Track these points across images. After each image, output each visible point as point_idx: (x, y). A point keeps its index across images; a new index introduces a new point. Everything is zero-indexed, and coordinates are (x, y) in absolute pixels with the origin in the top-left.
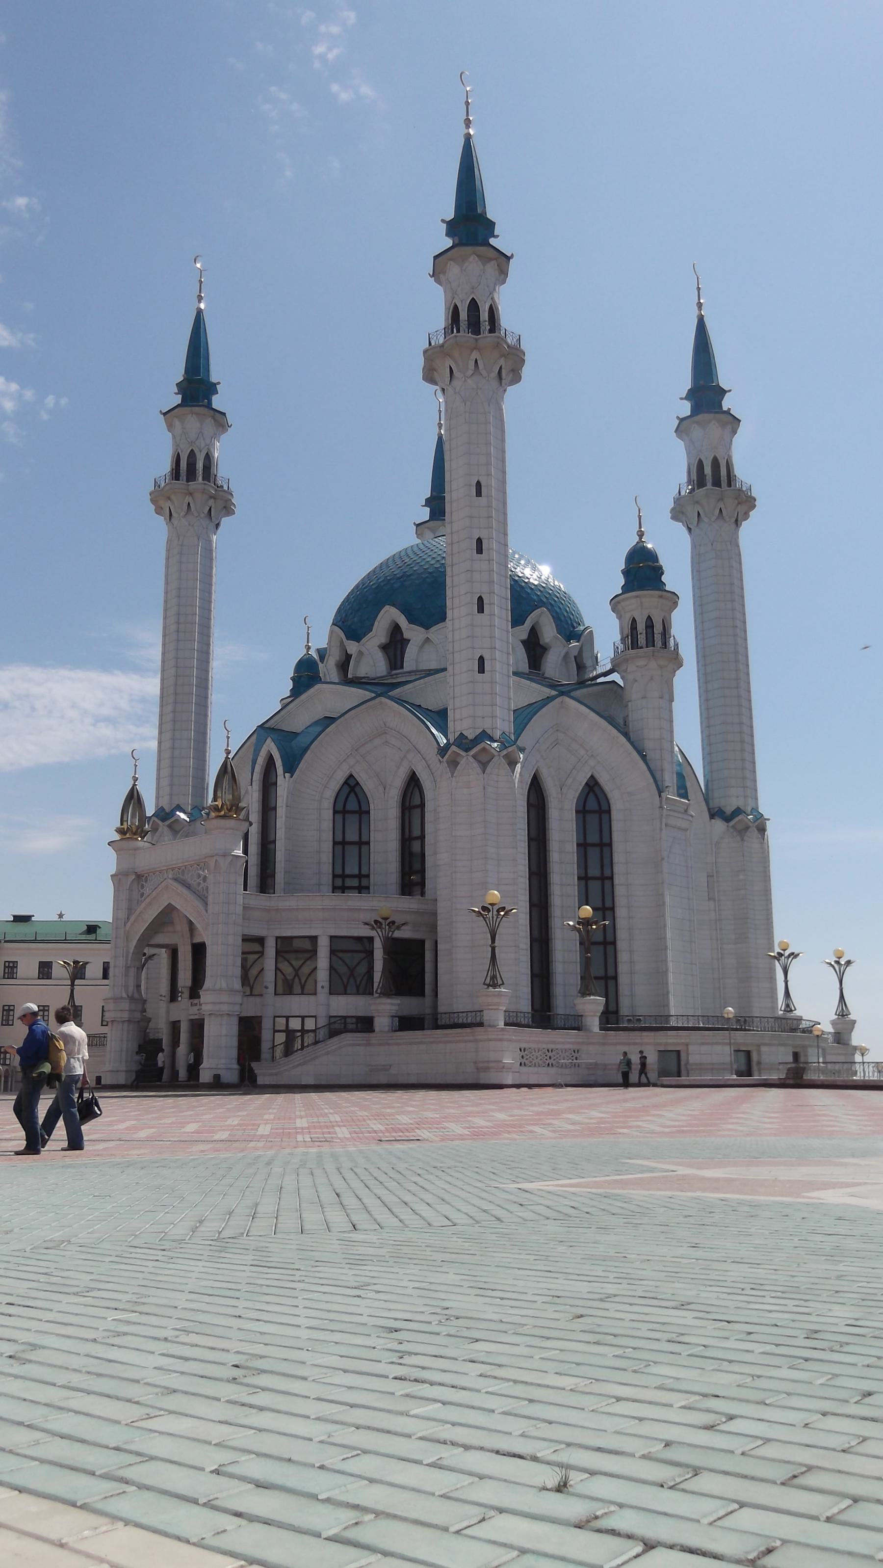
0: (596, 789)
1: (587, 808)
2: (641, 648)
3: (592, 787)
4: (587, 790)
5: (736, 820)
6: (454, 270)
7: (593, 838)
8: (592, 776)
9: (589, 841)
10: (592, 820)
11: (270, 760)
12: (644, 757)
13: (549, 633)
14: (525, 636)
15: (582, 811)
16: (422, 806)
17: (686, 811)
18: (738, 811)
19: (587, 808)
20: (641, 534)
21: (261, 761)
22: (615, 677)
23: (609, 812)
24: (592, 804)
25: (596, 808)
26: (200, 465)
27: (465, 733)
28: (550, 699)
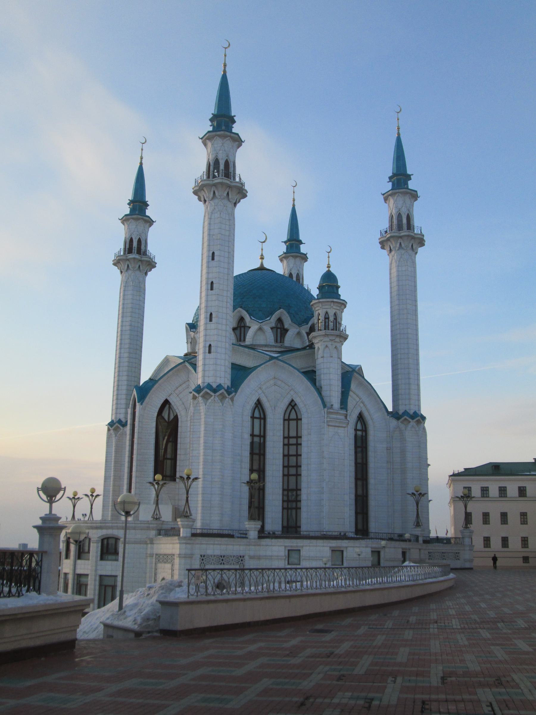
1: (291, 417)
2: (320, 330)
3: (292, 405)
4: (290, 407)
5: (403, 419)
6: (209, 144)
7: (293, 433)
8: (292, 400)
9: (291, 435)
12: (319, 390)
13: (287, 322)
14: (273, 325)
15: (287, 420)
17: (346, 417)
18: (405, 413)
19: (291, 417)
20: (329, 267)
24: (293, 416)
25: (295, 417)
26: (135, 244)
28: (269, 360)
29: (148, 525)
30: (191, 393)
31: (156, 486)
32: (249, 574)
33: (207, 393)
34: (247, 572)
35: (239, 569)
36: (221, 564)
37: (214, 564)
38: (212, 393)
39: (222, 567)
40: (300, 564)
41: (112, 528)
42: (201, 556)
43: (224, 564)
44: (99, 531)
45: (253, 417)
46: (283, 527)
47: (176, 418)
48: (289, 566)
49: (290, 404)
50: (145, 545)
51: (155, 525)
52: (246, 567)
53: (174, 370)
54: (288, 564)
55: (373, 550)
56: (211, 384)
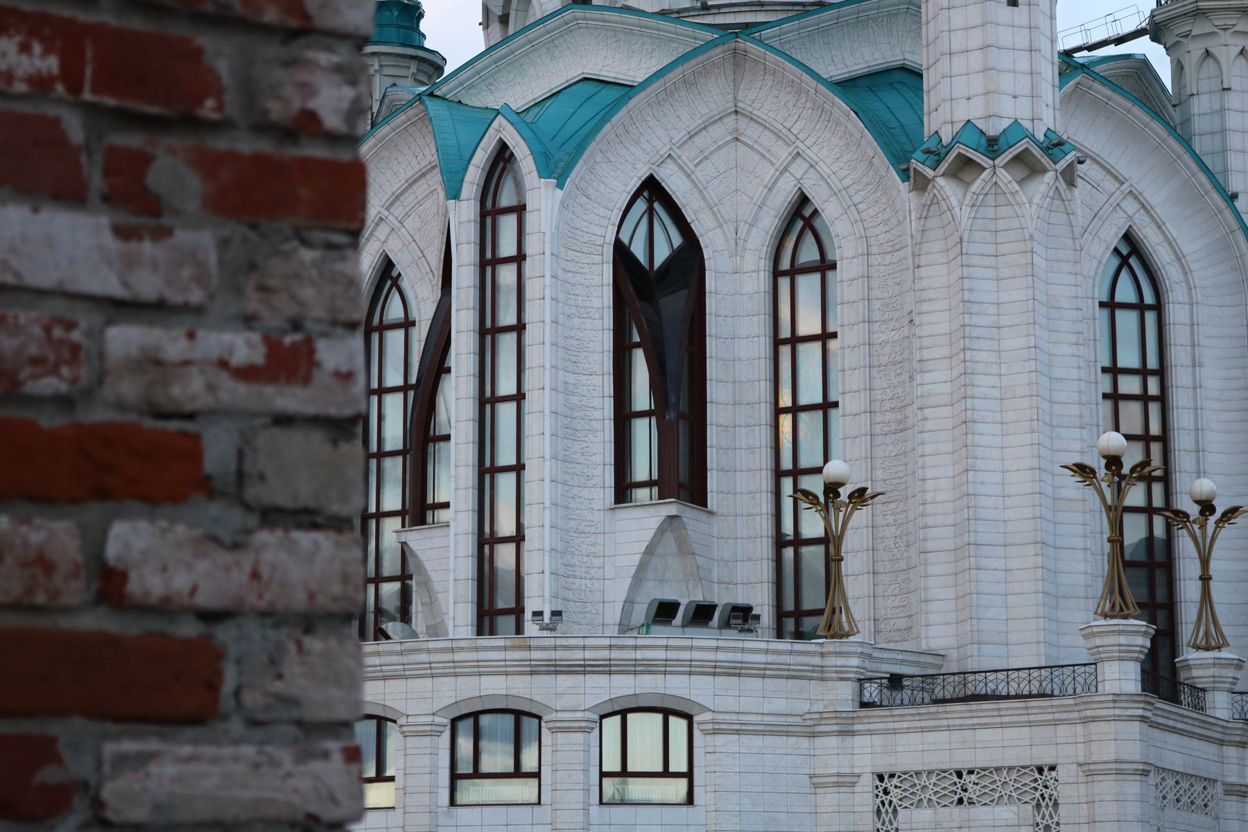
0: (1133, 261)
1: (1120, 297)
4: (1115, 262)
7: (1128, 357)
8: (1128, 237)
10: (1127, 321)
11: (503, 157)
15: (1111, 305)
16: (825, 266)
19: (1120, 297)
21: (481, 158)
22: (1143, 47)
23: (1158, 307)
24: (1125, 293)
25: (1131, 298)
27: (980, 124)
29: (816, 660)
33: (969, 162)
38: (1045, 160)
41: (665, 668)
44: (601, 680)
49: (1116, 251)
50: (805, 742)
51: (854, 662)
53: (693, 62)
56: (1027, 124)
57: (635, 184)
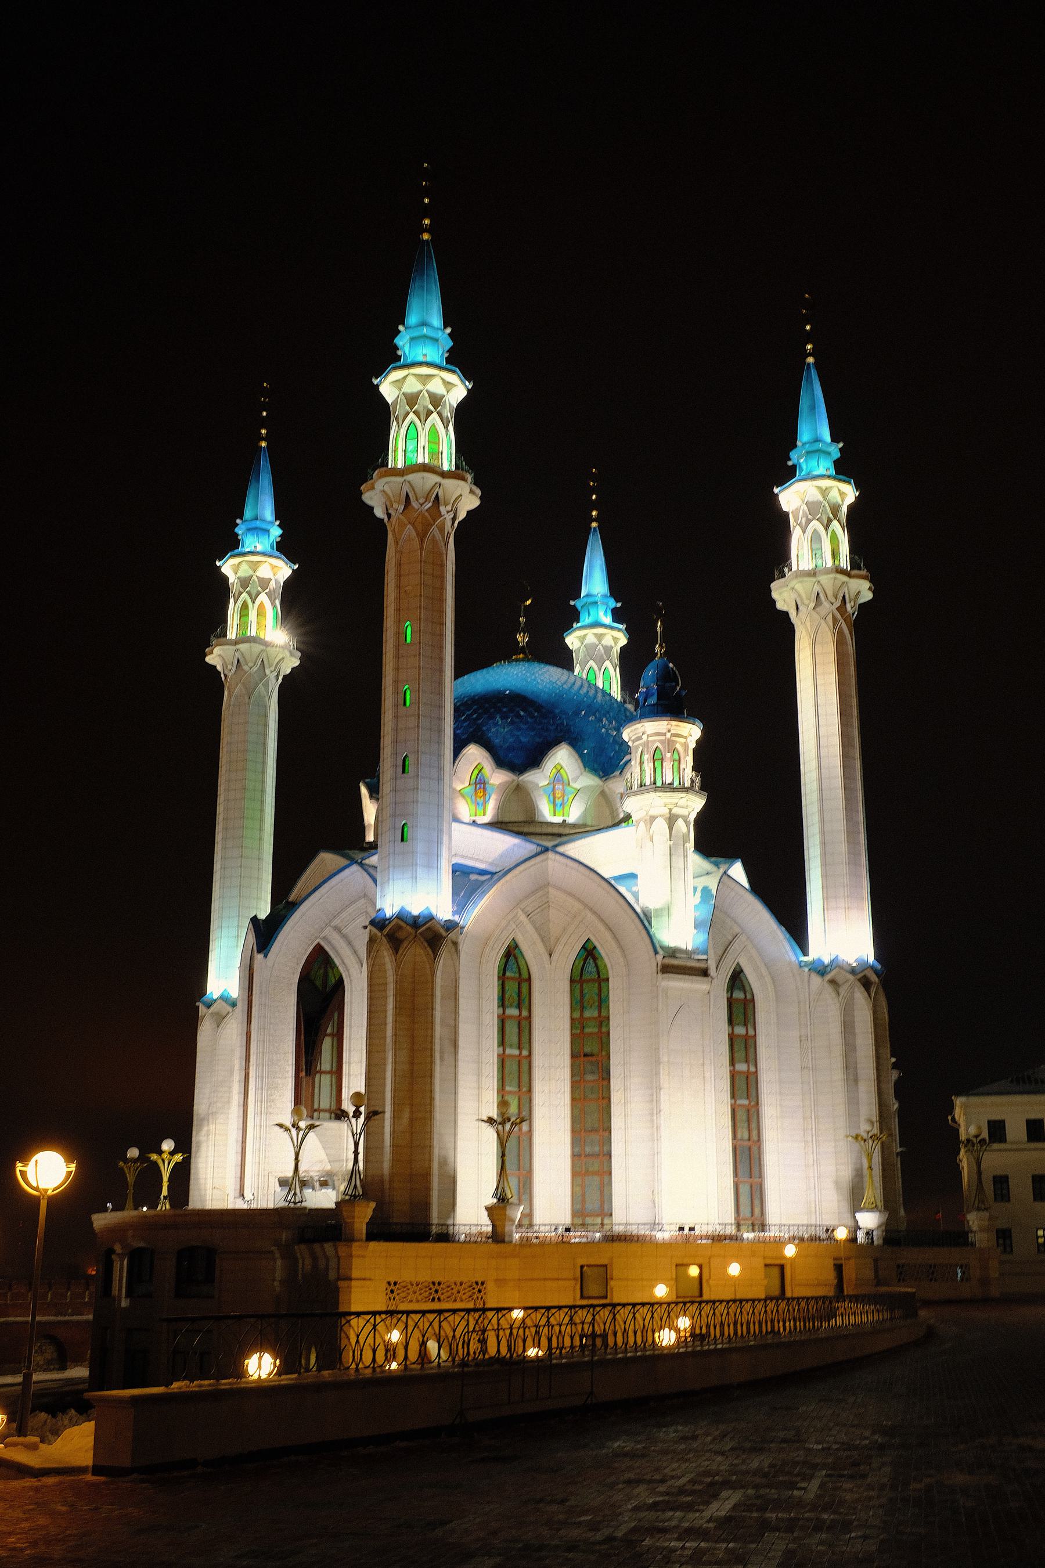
3: (589, 952)
15: (577, 980)
30: (365, 927)
31: (294, 1131)
32: (494, 1321)
34: (490, 1314)
35: (475, 1310)
36: (433, 1300)
37: (418, 1301)
39: (436, 1306)
40: (606, 1297)
42: (389, 1283)
43: (439, 1299)
45: (503, 979)
46: (574, 1214)
47: (340, 982)
48: (585, 1302)
49: (583, 947)
52: (488, 1306)
54: (582, 1297)
55: (769, 1262)
57: (311, 948)
